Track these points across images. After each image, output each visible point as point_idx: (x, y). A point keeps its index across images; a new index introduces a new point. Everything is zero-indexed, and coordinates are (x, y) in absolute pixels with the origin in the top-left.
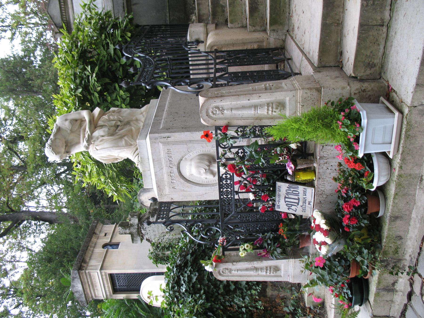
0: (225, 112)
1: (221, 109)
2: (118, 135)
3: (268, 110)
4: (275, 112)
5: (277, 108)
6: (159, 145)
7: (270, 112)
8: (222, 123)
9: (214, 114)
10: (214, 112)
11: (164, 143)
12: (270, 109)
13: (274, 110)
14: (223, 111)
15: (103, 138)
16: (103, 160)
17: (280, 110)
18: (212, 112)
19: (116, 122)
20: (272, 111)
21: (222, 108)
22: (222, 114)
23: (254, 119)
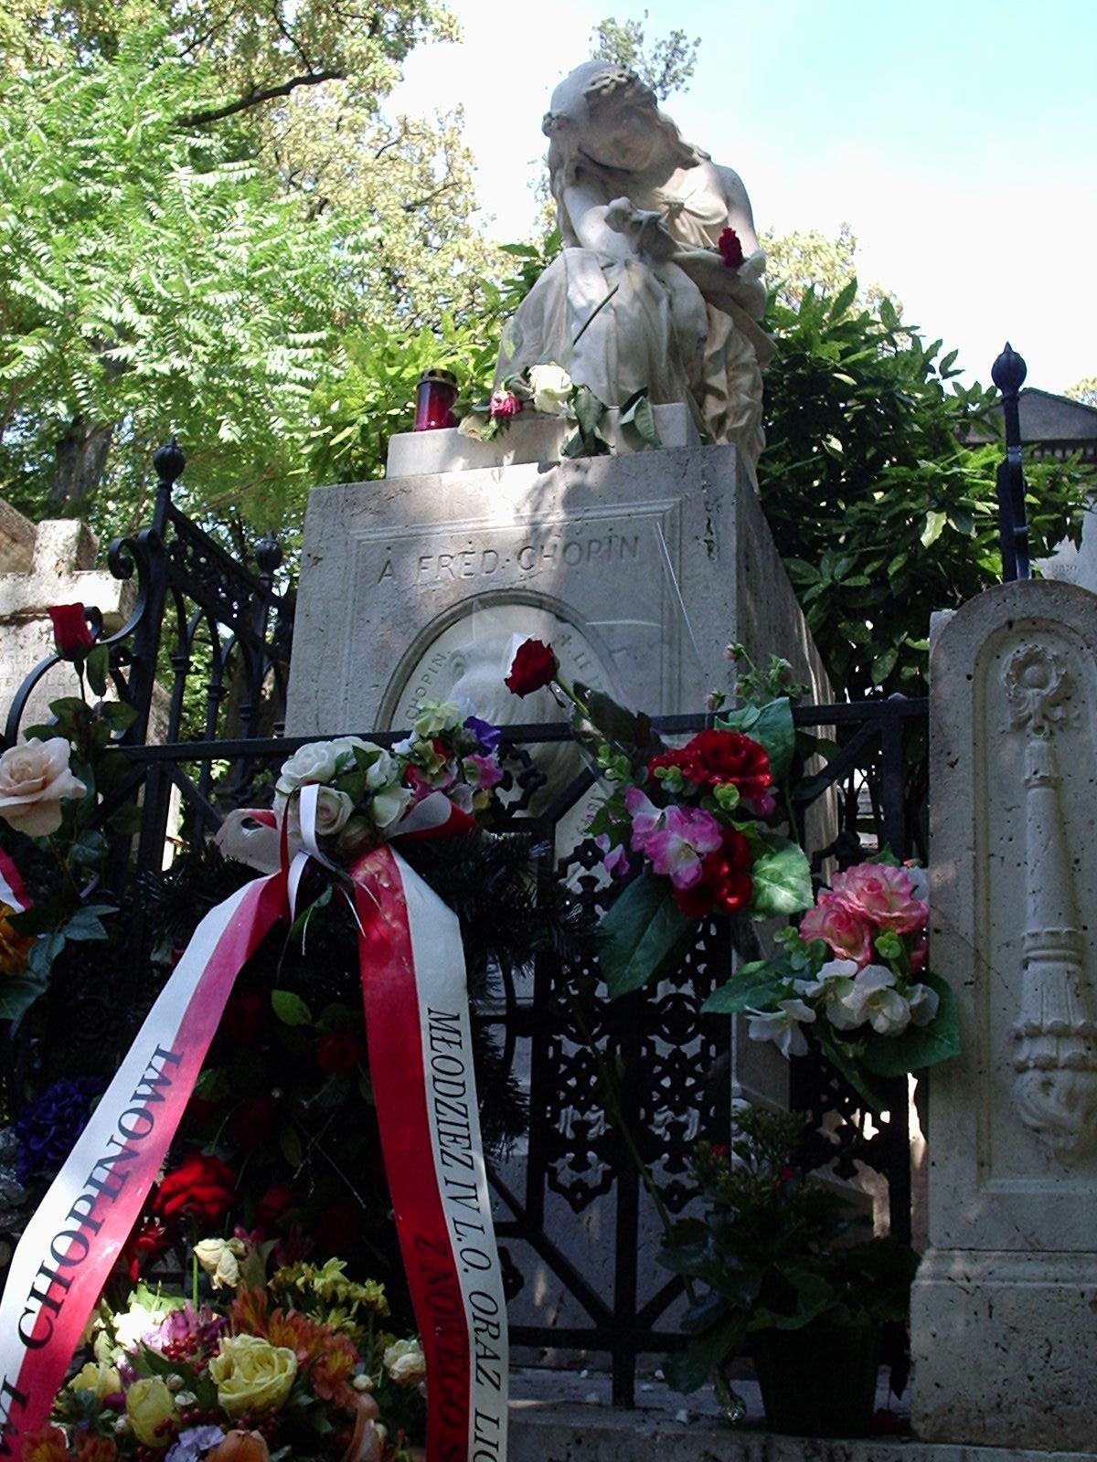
0: (1037, 743)
1: (1058, 713)
2: (670, 375)
3: (1061, 1033)
4: (1047, 1085)
5: (1071, 1099)
6: (667, 494)
7: (1043, 1048)
8: (949, 719)
9: (1020, 666)
10: (1031, 672)
11: (673, 523)
12: (1068, 1051)
13: (1062, 1078)
14: (1039, 729)
15: (664, 304)
16: (544, 297)
17: (1056, 1128)
18: (1033, 658)
19: (720, 395)
20: (1048, 1065)
21: (1063, 724)
22: (1020, 726)
23: (977, 935)
